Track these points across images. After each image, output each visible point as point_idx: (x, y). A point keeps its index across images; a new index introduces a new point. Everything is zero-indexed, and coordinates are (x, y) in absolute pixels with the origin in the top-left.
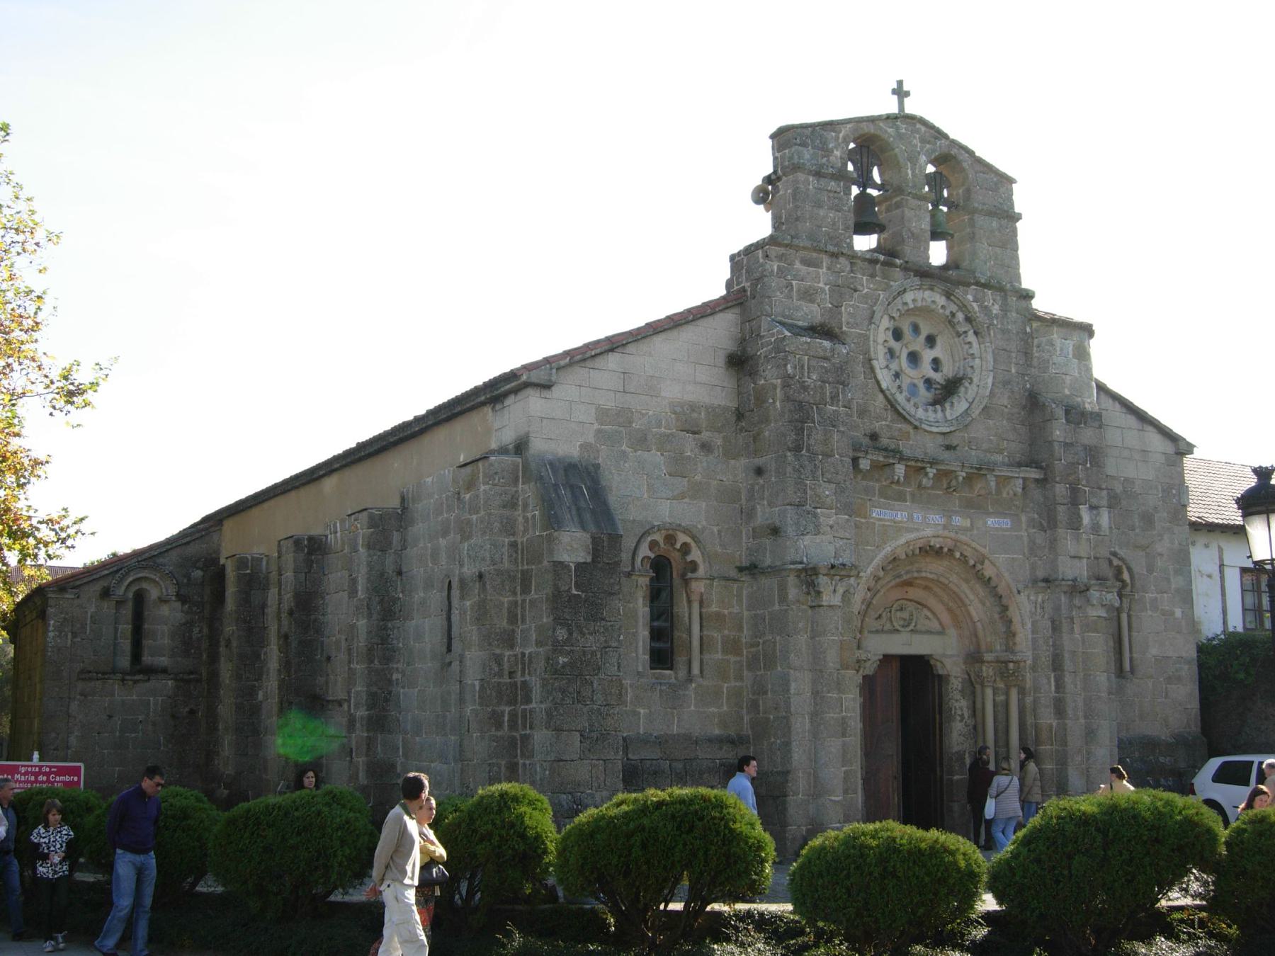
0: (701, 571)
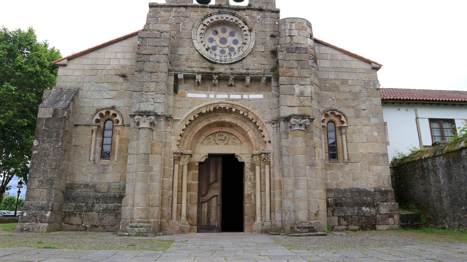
0: (120, 123)
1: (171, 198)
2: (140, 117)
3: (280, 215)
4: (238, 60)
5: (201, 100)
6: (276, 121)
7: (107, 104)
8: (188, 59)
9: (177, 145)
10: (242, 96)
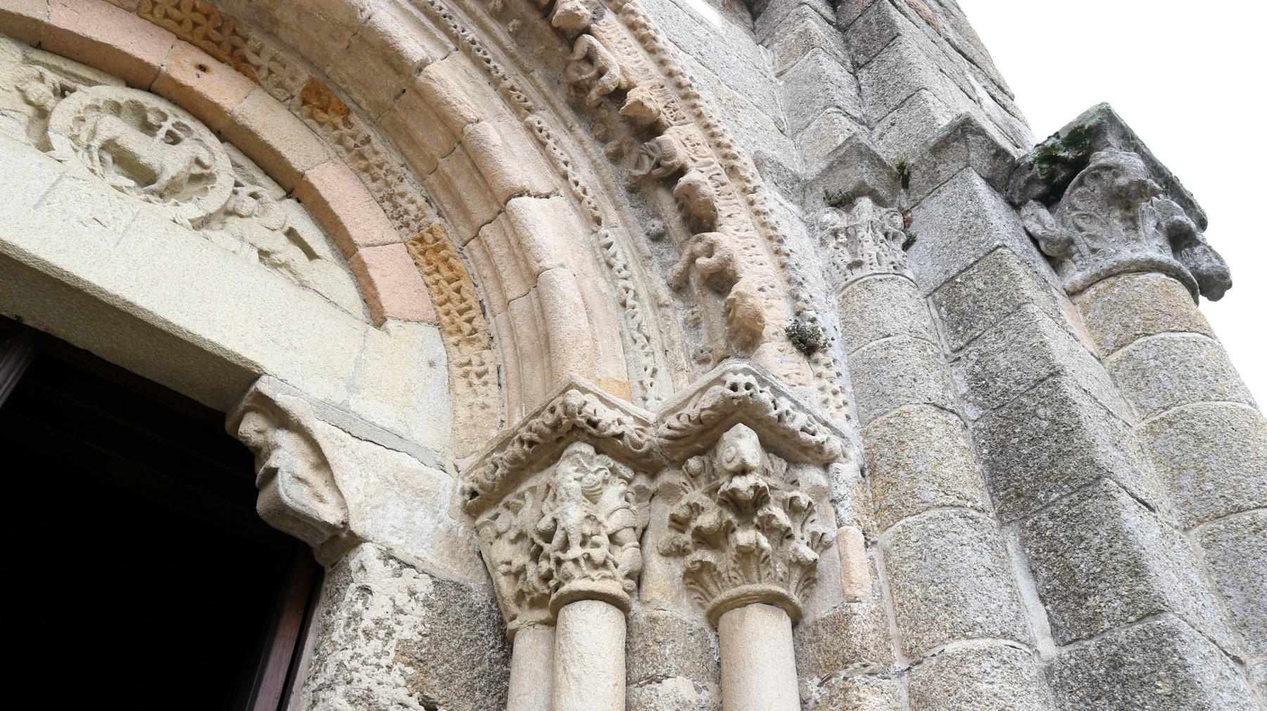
6: (879, 184)
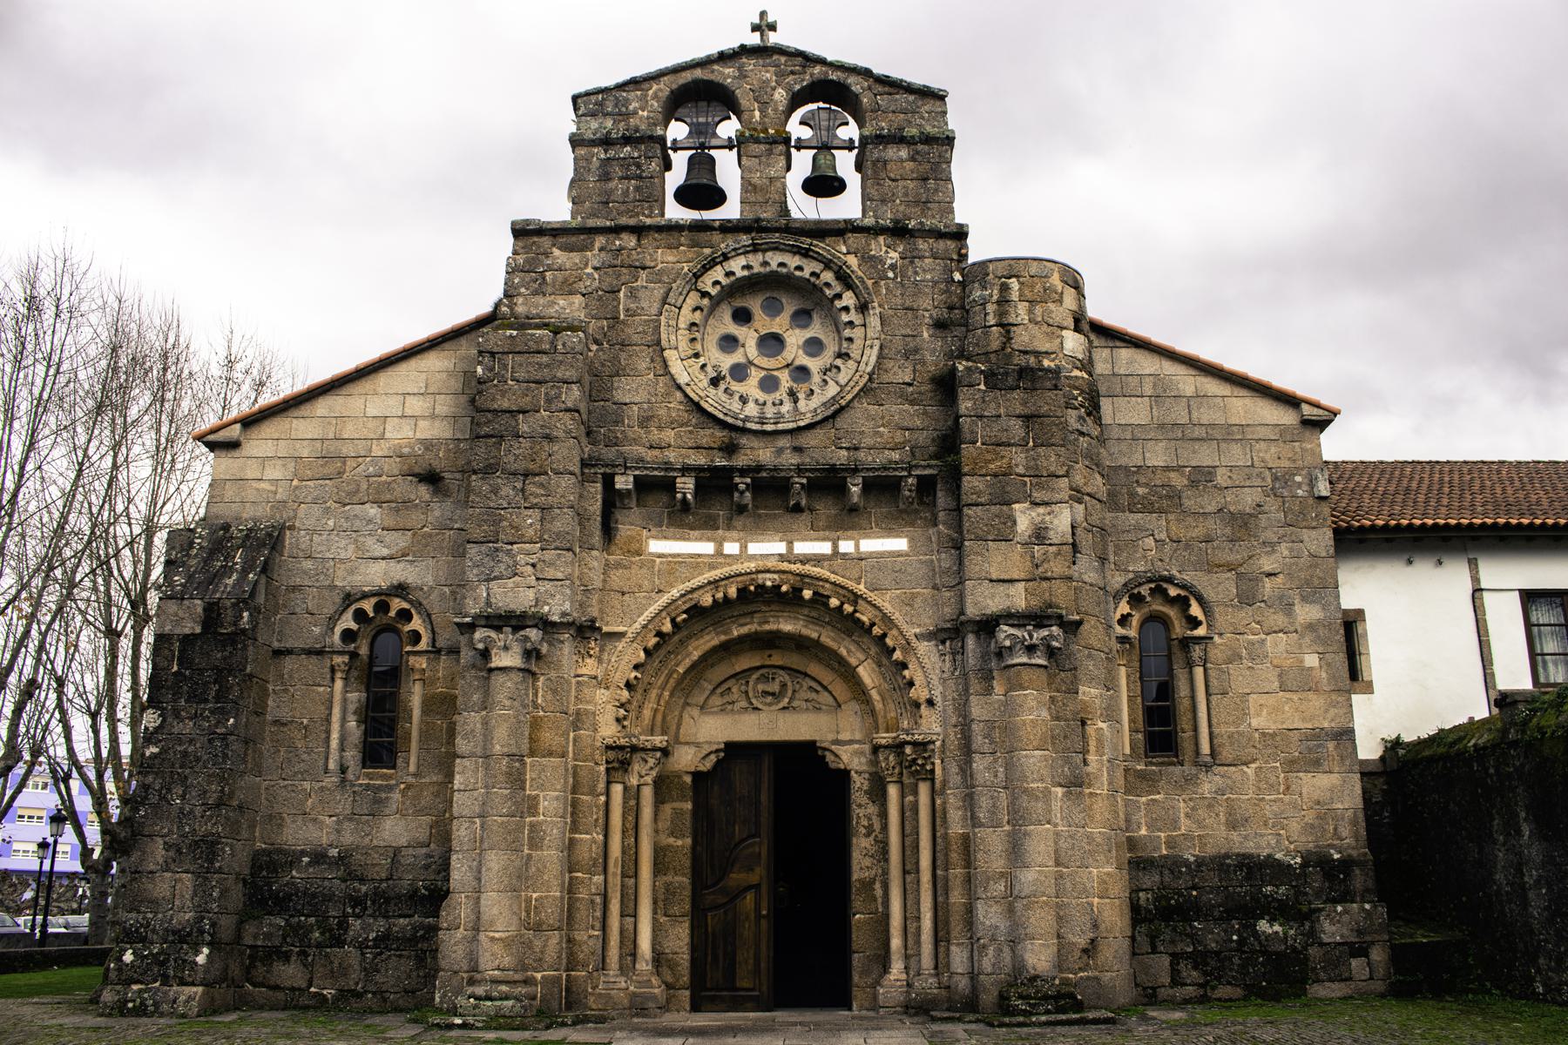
0: (423, 645)
1: (598, 900)
2: (493, 634)
3: (966, 954)
4: (819, 418)
5: (695, 562)
6: (951, 633)
7: (377, 575)
8: (649, 418)
9: (618, 720)
10: (835, 546)
